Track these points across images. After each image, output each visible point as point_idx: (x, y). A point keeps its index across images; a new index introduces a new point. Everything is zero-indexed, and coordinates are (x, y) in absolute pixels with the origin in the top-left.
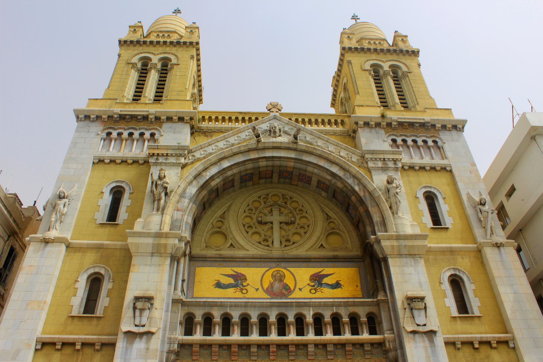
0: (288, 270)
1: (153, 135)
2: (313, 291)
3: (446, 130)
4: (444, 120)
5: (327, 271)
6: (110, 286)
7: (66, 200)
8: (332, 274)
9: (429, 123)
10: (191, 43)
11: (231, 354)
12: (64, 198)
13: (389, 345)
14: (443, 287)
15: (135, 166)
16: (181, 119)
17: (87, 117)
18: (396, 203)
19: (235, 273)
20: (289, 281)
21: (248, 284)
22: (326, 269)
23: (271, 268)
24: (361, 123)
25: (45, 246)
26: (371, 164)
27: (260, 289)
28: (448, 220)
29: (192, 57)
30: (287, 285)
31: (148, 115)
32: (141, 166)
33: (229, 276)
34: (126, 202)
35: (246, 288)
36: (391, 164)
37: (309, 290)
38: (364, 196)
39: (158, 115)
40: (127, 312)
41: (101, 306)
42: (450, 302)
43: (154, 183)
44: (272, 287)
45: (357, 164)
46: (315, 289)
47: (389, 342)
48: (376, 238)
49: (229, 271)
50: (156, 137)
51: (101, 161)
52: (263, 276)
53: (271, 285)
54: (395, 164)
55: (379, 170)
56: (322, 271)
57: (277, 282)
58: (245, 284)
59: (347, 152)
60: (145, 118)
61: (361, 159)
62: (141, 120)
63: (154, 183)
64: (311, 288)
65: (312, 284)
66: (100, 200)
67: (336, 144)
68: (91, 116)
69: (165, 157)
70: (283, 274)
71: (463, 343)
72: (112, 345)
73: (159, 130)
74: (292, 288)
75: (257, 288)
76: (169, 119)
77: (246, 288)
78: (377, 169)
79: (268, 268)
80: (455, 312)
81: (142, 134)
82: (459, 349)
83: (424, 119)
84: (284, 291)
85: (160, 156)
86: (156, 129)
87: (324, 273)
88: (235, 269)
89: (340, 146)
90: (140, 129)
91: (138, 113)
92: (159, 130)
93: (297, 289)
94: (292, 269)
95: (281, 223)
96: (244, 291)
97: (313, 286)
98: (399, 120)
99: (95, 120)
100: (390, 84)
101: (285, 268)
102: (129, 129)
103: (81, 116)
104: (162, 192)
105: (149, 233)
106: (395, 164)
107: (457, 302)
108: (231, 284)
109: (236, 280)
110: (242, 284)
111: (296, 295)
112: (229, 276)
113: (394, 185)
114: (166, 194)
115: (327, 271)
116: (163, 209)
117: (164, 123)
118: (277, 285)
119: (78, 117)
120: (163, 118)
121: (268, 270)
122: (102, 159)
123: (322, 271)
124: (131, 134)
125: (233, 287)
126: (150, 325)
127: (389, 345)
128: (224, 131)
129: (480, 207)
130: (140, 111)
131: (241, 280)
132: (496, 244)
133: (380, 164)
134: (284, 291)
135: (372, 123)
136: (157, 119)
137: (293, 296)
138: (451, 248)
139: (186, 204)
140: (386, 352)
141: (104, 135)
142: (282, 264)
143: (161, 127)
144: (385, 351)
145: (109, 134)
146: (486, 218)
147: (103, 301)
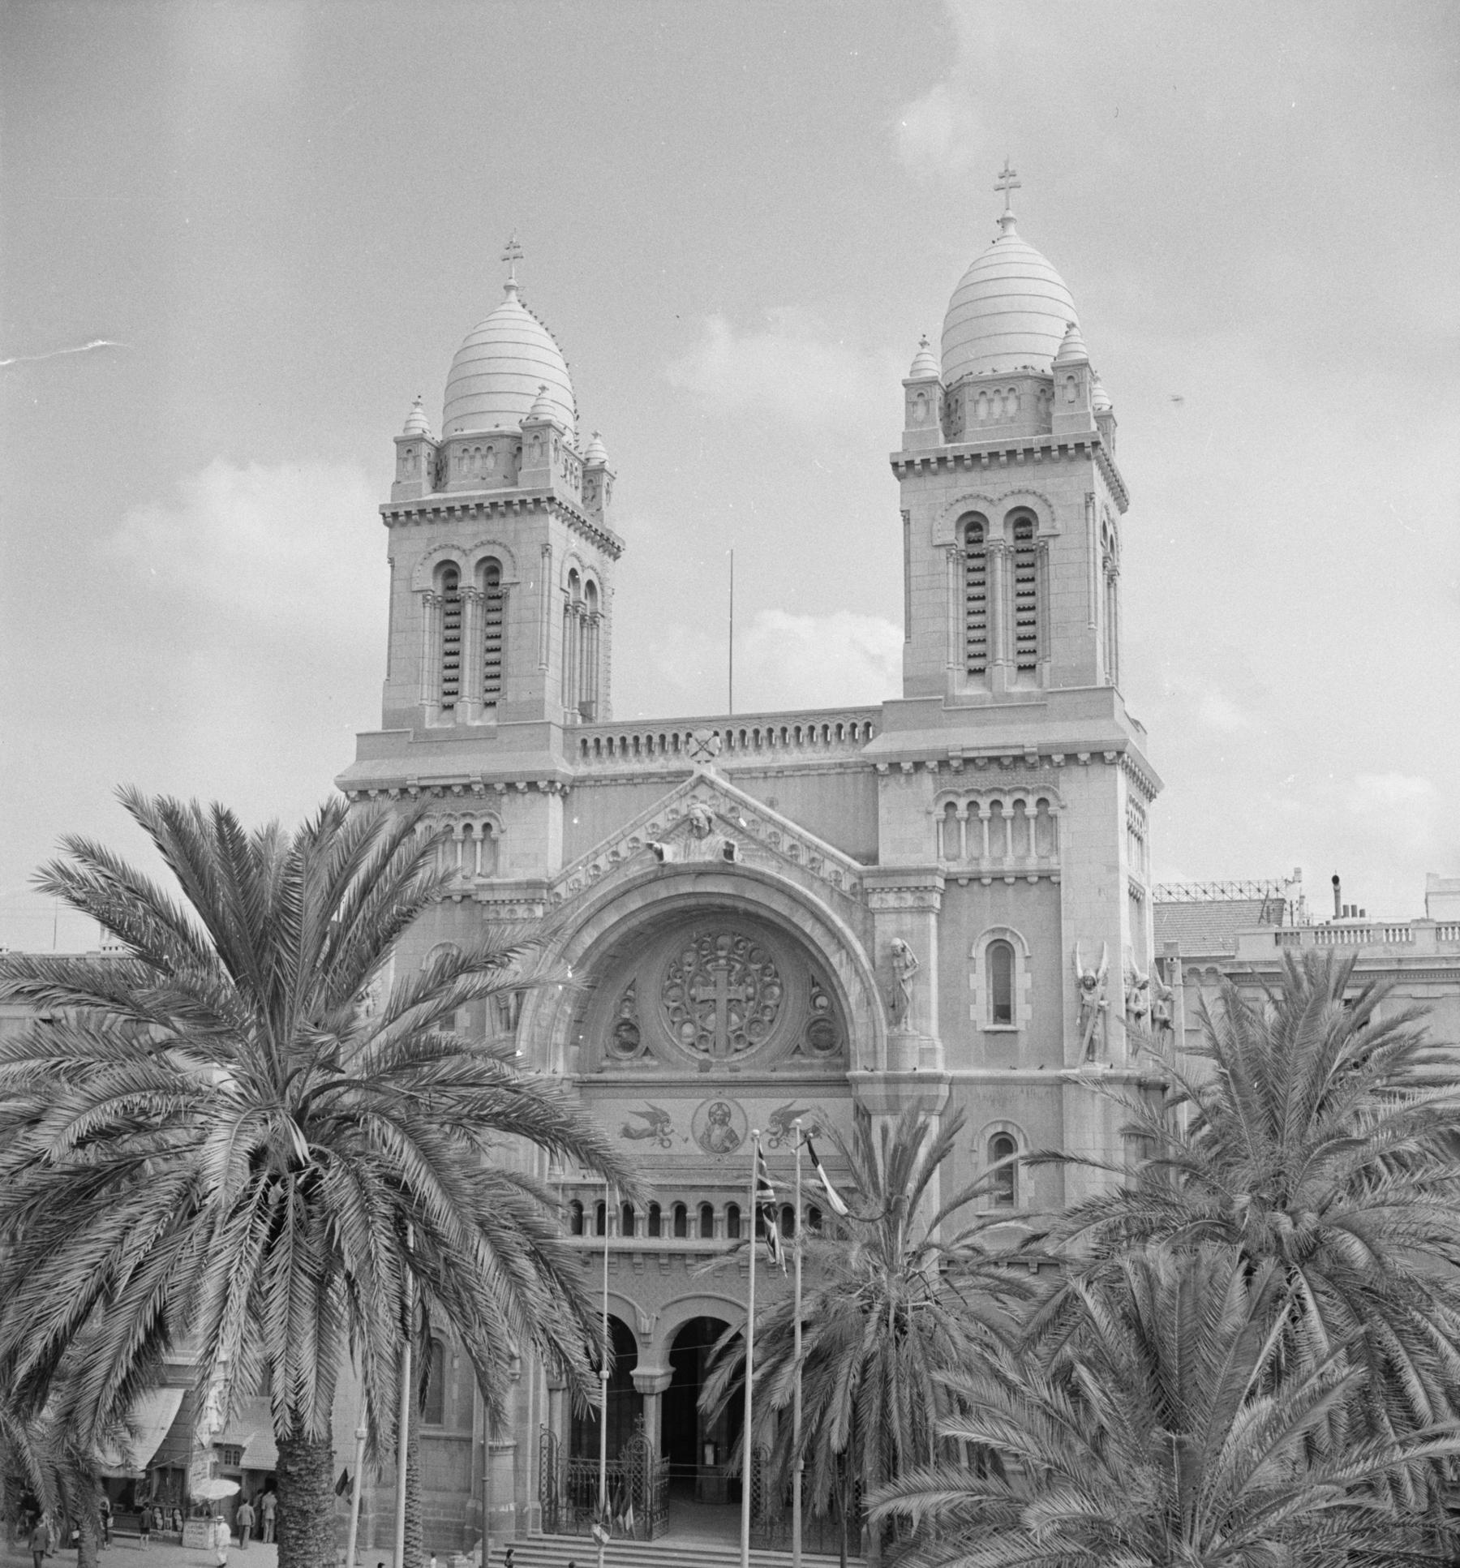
0: (737, 1104)
2: (774, 1144)
3: (1078, 764)
5: (800, 1104)
8: (808, 1111)
11: (635, 1266)
14: (975, 1158)
19: (651, 1110)
20: (735, 1123)
21: (672, 1131)
22: (800, 1101)
23: (709, 1099)
27: (691, 1137)
28: (1022, 1012)
30: (732, 1131)
33: (642, 1115)
35: (670, 1137)
37: (767, 1140)
44: (709, 1136)
46: (778, 1140)
49: (641, 1105)
50: (494, 833)
52: (696, 1113)
53: (708, 1134)
56: (791, 1104)
57: (717, 1126)
58: (667, 1130)
64: (770, 1137)
65: (774, 1130)
70: (726, 1110)
73: (496, 818)
74: (740, 1137)
75: (685, 1136)
77: (670, 1137)
79: (701, 1100)
83: (1023, 747)
84: (728, 1144)
87: (792, 1108)
88: (653, 1102)
92: (496, 818)
93: (748, 1142)
94: (740, 1101)
95: (730, 1001)
96: (666, 1143)
97: (775, 1134)
100: (1002, 574)
101: (731, 1099)
108: (645, 1130)
109: (653, 1123)
110: (662, 1131)
111: (747, 1149)
112: (642, 1115)
115: (800, 1104)
116: (516, 1023)
118: (718, 1132)
121: (702, 1104)
123: (791, 1104)
125: (648, 1136)
131: (662, 1122)
134: (728, 1144)
137: (741, 1152)
142: (727, 1092)
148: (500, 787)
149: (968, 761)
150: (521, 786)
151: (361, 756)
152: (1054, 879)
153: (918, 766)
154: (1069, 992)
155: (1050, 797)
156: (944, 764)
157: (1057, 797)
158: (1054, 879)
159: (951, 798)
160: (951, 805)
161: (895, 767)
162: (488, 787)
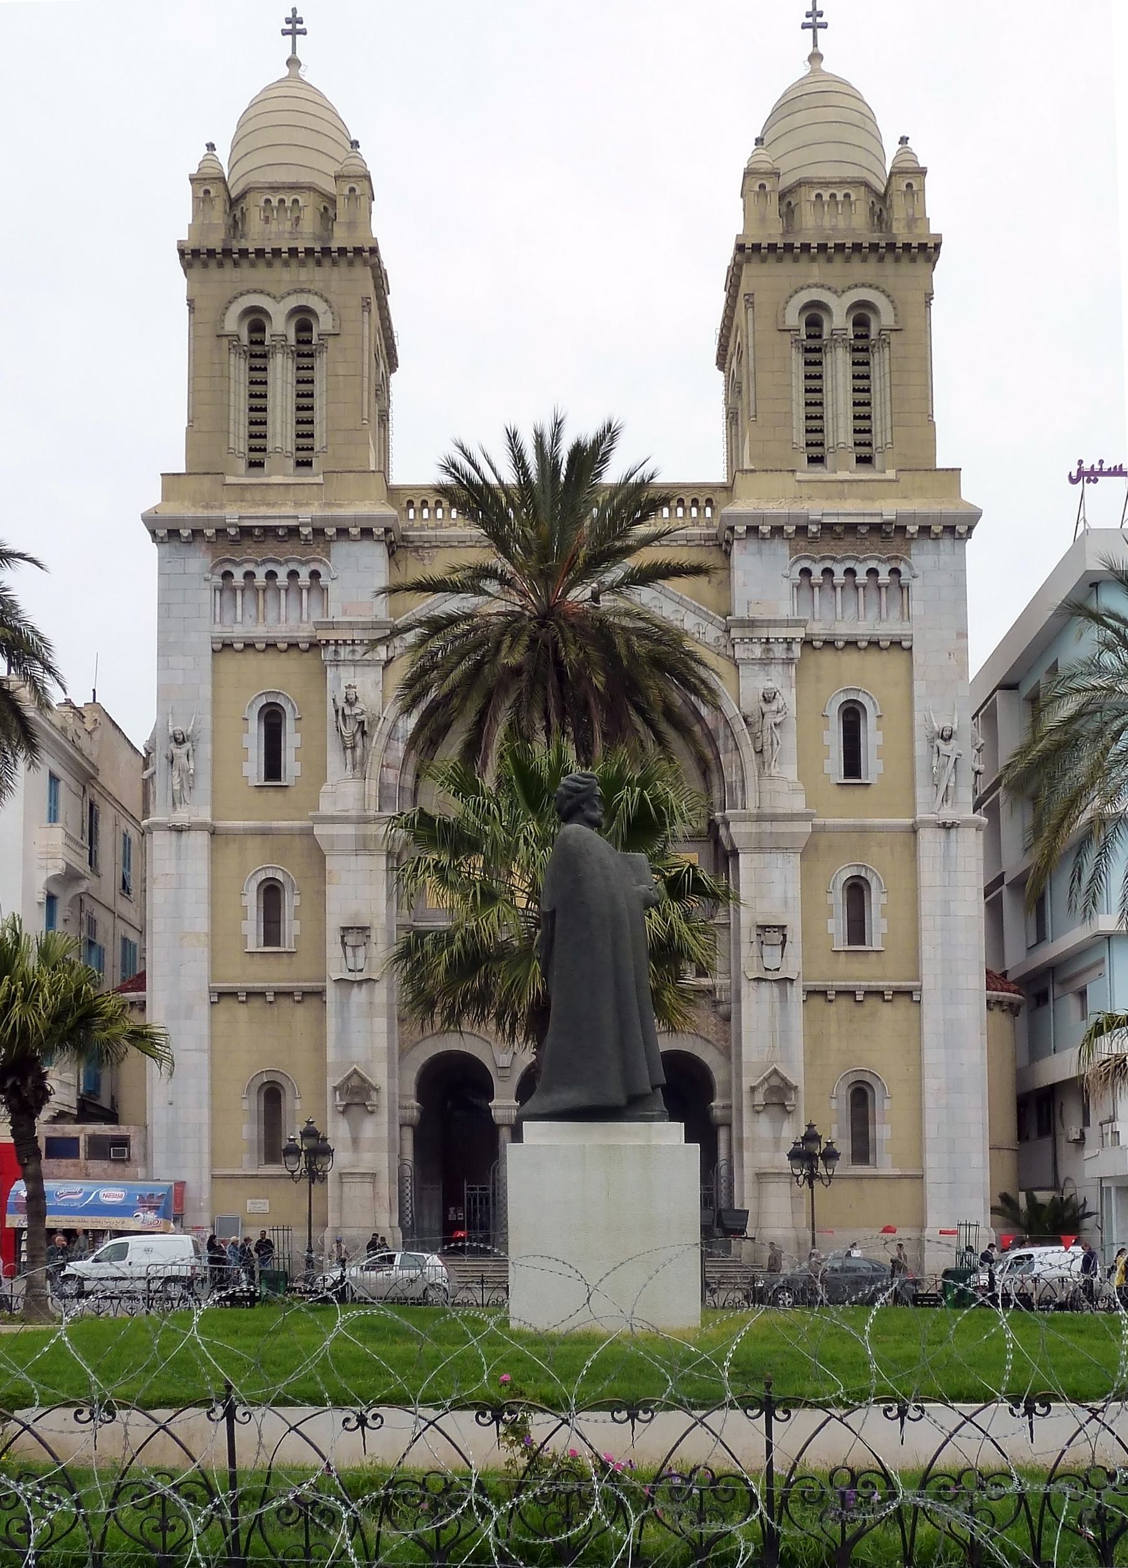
1: (315, 575)
4: (927, 516)
6: (297, 901)
7: (188, 745)
9: (890, 524)
10: (358, 251)
12: (184, 741)
13: (720, 995)
14: (830, 899)
15: (294, 654)
16: (367, 533)
17: (173, 533)
18: (772, 745)
24: (741, 529)
25: (179, 839)
26: (740, 652)
29: (366, 305)
31: (298, 527)
32: (305, 655)
34: (291, 740)
36: (779, 651)
38: (717, 729)
39: (318, 525)
40: (334, 950)
41: (290, 934)
42: (837, 926)
43: (340, 713)
45: (713, 649)
47: (720, 991)
48: (723, 817)
50: (323, 581)
51: (227, 646)
54: (789, 649)
55: (754, 664)
59: (700, 620)
60: (293, 532)
61: (723, 636)
62: (286, 539)
63: (340, 713)
66: (245, 735)
67: (678, 600)
68: (181, 531)
69: (351, 648)
71: (839, 993)
72: (319, 994)
73: (325, 564)
76: (343, 532)
78: (753, 661)
80: (840, 943)
81: (293, 575)
82: (831, 1001)
83: (881, 515)
85: (340, 645)
86: (320, 561)
89: (685, 603)
90: (287, 561)
91: (277, 523)
92: (325, 564)
98: (826, 520)
99: (191, 540)
102: (264, 562)
103: (162, 533)
104: (357, 731)
105: (347, 818)
106: (789, 649)
107: (850, 921)
113: (774, 707)
114: (364, 733)
117: (332, 545)
119: (153, 533)
120: (331, 531)
122: (228, 642)
124: (271, 575)
126: (370, 971)
127: (720, 995)
128: (456, 544)
129: (939, 742)
130: (280, 517)
132: (944, 823)
133: (758, 651)
135: (765, 529)
136: (318, 532)
138: (862, 826)
139: (401, 754)
140: (717, 1004)
141: (218, 580)
143: (328, 556)
144: (714, 1001)
145: (227, 575)
146: (944, 767)
147: (291, 927)
148: (331, 531)
149: (827, 528)
150: (354, 531)
151: (166, 497)
152: (905, 644)
153: (777, 531)
154: (921, 748)
155: (902, 567)
156: (802, 530)
157: (910, 567)
158: (905, 644)
159: (806, 564)
160: (806, 572)
161: (753, 530)
162: (318, 532)
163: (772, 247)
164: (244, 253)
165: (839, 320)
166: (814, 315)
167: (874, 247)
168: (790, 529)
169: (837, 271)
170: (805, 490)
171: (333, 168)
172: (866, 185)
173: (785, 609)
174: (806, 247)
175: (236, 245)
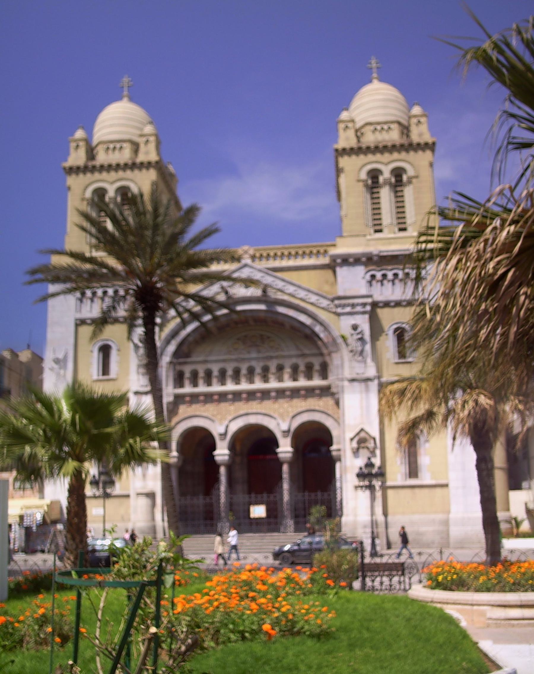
24: (339, 261)
98: (382, 254)
135: (351, 260)
160: (373, 277)
163: (352, 149)
164: (94, 167)
165: (386, 174)
166: (374, 174)
167: (402, 146)
168: (364, 259)
169: (387, 157)
170: (372, 242)
171: (139, 132)
172: (399, 123)
173: (364, 291)
174: (368, 148)
175: (90, 164)
